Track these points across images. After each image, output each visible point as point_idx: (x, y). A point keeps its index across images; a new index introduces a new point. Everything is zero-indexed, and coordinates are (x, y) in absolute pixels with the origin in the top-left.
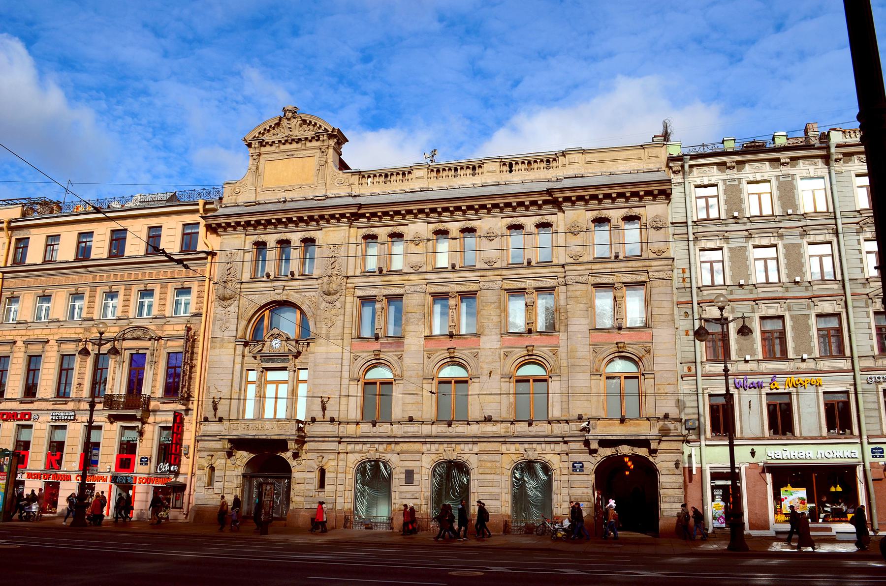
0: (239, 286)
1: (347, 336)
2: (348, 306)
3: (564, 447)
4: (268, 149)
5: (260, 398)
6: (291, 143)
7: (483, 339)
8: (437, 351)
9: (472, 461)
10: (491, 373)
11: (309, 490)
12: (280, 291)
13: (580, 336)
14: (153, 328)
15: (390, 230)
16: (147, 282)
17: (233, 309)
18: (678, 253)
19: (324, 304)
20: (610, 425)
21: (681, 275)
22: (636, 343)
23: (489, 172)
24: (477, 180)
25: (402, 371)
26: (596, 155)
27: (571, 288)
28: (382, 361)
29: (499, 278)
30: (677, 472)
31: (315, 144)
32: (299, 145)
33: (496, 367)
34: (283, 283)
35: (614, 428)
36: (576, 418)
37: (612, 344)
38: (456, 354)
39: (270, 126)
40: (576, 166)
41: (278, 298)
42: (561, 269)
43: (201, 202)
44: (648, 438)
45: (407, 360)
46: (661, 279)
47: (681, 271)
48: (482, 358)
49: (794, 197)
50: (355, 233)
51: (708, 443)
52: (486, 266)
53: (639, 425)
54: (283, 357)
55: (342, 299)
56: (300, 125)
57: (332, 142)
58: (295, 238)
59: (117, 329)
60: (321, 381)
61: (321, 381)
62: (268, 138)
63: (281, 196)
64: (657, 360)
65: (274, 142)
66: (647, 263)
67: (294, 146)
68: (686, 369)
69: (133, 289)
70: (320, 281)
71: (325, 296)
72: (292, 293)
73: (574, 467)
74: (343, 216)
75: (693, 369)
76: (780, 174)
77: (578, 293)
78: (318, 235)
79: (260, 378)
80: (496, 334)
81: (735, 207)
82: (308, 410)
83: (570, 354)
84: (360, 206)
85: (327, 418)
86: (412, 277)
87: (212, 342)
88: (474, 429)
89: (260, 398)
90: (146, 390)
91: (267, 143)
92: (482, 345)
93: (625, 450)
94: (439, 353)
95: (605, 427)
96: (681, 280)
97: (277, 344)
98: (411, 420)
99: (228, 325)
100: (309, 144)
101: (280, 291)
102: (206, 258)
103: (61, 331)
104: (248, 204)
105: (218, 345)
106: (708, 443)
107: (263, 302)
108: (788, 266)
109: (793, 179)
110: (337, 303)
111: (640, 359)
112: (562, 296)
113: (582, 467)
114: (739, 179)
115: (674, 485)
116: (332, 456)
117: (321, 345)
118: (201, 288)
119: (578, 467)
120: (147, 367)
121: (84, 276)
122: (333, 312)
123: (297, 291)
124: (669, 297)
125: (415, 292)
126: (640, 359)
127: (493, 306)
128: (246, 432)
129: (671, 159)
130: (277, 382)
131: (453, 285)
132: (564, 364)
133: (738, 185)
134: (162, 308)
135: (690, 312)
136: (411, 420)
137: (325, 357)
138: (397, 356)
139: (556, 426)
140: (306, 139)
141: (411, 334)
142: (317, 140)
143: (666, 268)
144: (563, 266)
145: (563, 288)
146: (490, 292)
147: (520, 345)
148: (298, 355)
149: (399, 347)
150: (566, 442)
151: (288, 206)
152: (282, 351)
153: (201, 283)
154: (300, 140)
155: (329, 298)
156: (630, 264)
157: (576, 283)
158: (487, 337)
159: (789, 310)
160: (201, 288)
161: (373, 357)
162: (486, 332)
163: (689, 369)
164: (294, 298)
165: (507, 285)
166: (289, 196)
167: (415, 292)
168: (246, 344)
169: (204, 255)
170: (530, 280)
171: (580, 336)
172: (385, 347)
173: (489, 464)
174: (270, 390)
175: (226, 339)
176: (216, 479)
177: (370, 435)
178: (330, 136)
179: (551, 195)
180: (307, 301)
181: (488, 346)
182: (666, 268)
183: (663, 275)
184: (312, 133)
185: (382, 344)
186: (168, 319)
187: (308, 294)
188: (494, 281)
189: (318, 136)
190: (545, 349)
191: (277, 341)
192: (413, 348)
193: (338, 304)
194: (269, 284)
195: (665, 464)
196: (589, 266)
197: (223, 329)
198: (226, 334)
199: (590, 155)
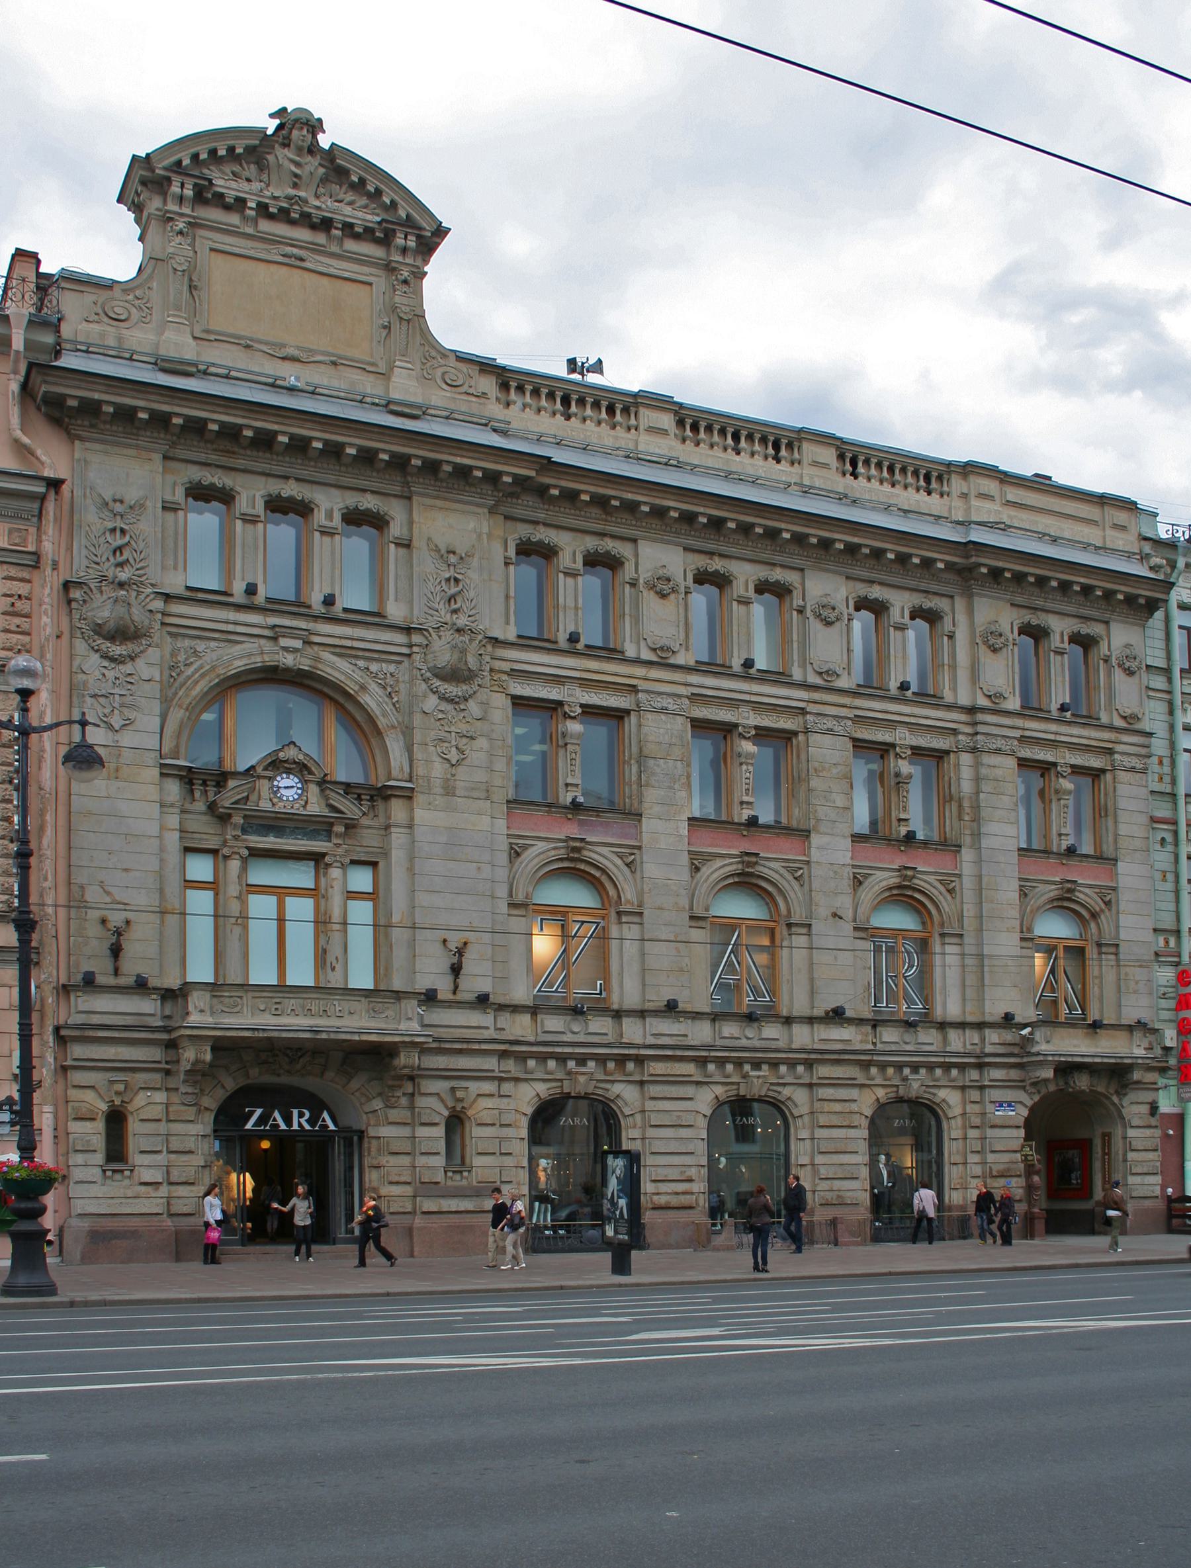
0: (159, 604)
1: (501, 796)
3: (974, 1074)
4: (214, 214)
5: (229, 924)
6: (292, 222)
10: (835, 915)
12: (298, 644)
17: (148, 665)
25: (640, 894)
27: (987, 759)
28: (582, 866)
29: (850, 713)
30: (1153, 1121)
31: (377, 252)
32: (321, 238)
33: (844, 903)
34: (303, 624)
41: (289, 660)
42: (963, 717)
45: (651, 869)
52: (818, 681)
55: (483, 695)
56: (324, 180)
62: (224, 183)
64: (1124, 921)
65: (241, 203)
67: (302, 234)
68: (1161, 942)
70: (416, 638)
71: (437, 682)
72: (326, 655)
75: (1172, 943)
80: (844, 836)
88: (802, 1036)
89: (229, 924)
92: (815, 855)
94: (719, 863)
99: (132, 715)
100: (351, 245)
101: (298, 644)
107: (239, 665)
111: (1094, 916)
112: (966, 773)
116: (488, 1087)
122: (463, 728)
123: (343, 652)
125: (664, 710)
126: (1094, 916)
127: (834, 771)
130: (281, 893)
131: (744, 709)
132: (969, 911)
135: (1169, 838)
137: (443, 839)
138: (621, 856)
139: (953, 1035)
140: (348, 228)
142: (378, 241)
144: (972, 710)
145: (966, 758)
146: (827, 740)
150: (980, 1066)
154: (325, 225)
155: (452, 689)
161: (562, 853)
164: (338, 669)
167: (664, 710)
168: (189, 778)
173: (837, 1107)
174: (262, 906)
177: (565, 1038)
180: (373, 687)
183: (1136, 762)
191: (292, 781)
193: (473, 707)
195: (1136, 1109)
196: (1019, 722)
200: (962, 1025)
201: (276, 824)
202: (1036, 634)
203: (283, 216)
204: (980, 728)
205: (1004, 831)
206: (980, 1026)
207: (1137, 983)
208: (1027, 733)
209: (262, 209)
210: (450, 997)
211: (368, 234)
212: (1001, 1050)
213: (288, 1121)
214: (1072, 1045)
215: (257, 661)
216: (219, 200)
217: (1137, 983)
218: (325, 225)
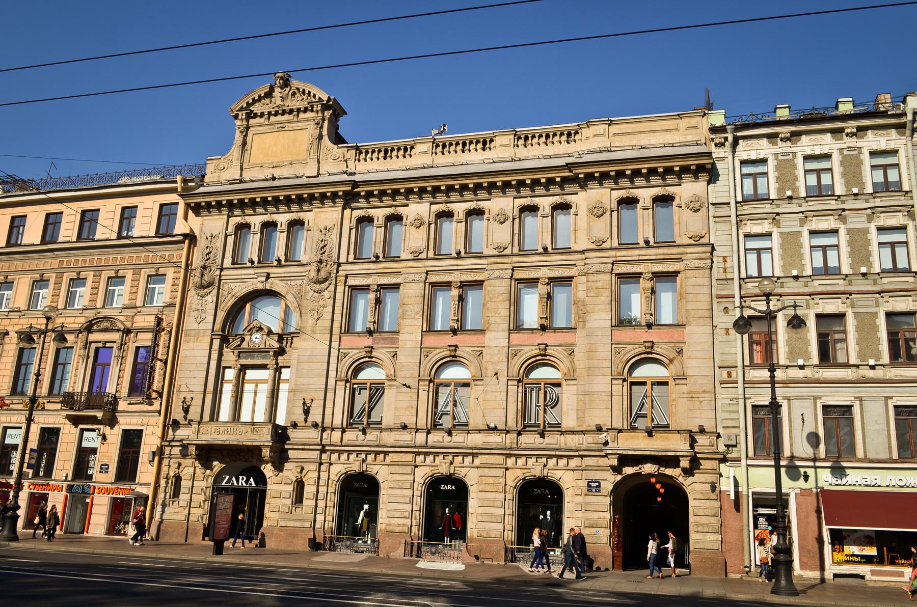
2: (339, 296)
4: (258, 120)
6: (283, 114)
7: (488, 335)
8: (435, 348)
9: (471, 478)
10: (496, 374)
11: (284, 505)
13: (600, 333)
14: (122, 318)
15: (389, 211)
16: (118, 268)
18: (719, 238)
19: (311, 293)
20: (632, 437)
21: (722, 265)
22: (666, 343)
23: (502, 146)
24: (488, 155)
26: (625, 126)
27: (591, 278)
30: (713, 496)
31: (309, 115)
32: (291, 117)
34: (267, 270)
35: (636, 441)
36: (594, 428)
37: (638, 343)
38: (458, 353)
39: (260, 96)
40: (600, 138)
41: (260, 286)
43: (179, 178)
44: (678, 454)
45: (401, 357)
46: (697, 268)
47: (721, 259)
48: (486, 357)
49: (860, 173)
50: (352, 215)
51: (750, 462)
53: (667, 438)
54: (263, 352)
57: (328, 114)
58: (282, 219)
59: (82, 320)
60: (304, 381)
61: (304, 381)
62: (257, 108)
63: (268, 173)
66: (681, 250)
67: (286, 117)
68: (725, 374)
69: (103, 276)
70: (307, 268)
72: (276, 281)
73: (589, 486)
74: (335, 195)
76: (845, 146)
77: (599, 284)
78: (306, 216)
79: (238, 377)
81: (788, 185)
82: (289, 413)
83: (591, 352)
84: (355, 184)
85: (309, 423)
86: (411, 264)
87: (186, 335)
90: (111, 389)
91: (256, 114)
93: (648, 468)
94: (438, 351)
95: (627, 440)
96: (721, 270)
97: (257, 339)
98: (404, 427)
100: (302, 115)
102: (183, 242)
103: (22, 321)
104: (231, 182)
105: (192, 338)
106: (750, 462)
108: (851, 254)
109: (860, 153)
110: (326, 293)
112: (582, 287)
113: (599, 486)
114: (794, 154)
115: (709, 512)
117: (305, 340)
118: (177, 275)
119: (593, 487)
120: (113, 362)
121: (49, 261)
122: (321, 303)
123: (282, 278)
124: (706, 290)
125: (413, 281)
127: (501, 298)
128: (215, 436)
129: (714, 130)
130: (257, 382)
131: (457, 273)
133: (793, 160)
134: (133, 296)
136: (404, 427)
137: (309, 353)
139: (569, 437)
140: (299, 110)
141: (407, 329)
143: (703, 255)
144: (583, 252)
145: (584, 279)
147: (532, 343)
148: (281, 352)
149: (393, 343)
151: (277, 183)
152: (263, 346)
153: (177, 269)
154: (291, 112)
156: (661, 251)
157: (598, 272)
158: (494, 333)
159: (853, 306)
160: (177, 275)
162: (492, 327)
163: (729, 375)
164: (276, 285)
165: (519, 275)
166: (277, 173)
169: (181, 238)
170: (545, 270)
171: (600, 333)
172: (378, 343)
173: (491, 480)
174: (249, 388)
175: (202, 332)
176: (182, 490)
178: (325, 107)
179: (571, 171)
181: (493, 343)
182: (703, 255)
184: (305, 104)
185: (374, 339)
186: (139, 309)
187: (293, 283)
188: (503, 268)
189: (312, 106)
190: (559, 348)
191: (258, 335)
192: (409, 345)
193: (326, 294)
194: (251, 271)
195: (697, 486)
196: (612, 253)
197: (199, 320)
198: (202, 326)
199: (618, 126)
200: (573, 432)
201: (251, 352)
202: (630, 202)
203: (276, 114)
204: (588, 261)
205: (601, 318)
206: (583, 432)
207: (701, 402)
208: (618, 259)
209: (270, 113)
210: (304, 424)
211: (306, 110)
212: (594, 447)
213: (238, 483)
214: (638, 444)
215: (251, 289)
216: (255, 116)
217: (701, 402)
218: (291, 112)
